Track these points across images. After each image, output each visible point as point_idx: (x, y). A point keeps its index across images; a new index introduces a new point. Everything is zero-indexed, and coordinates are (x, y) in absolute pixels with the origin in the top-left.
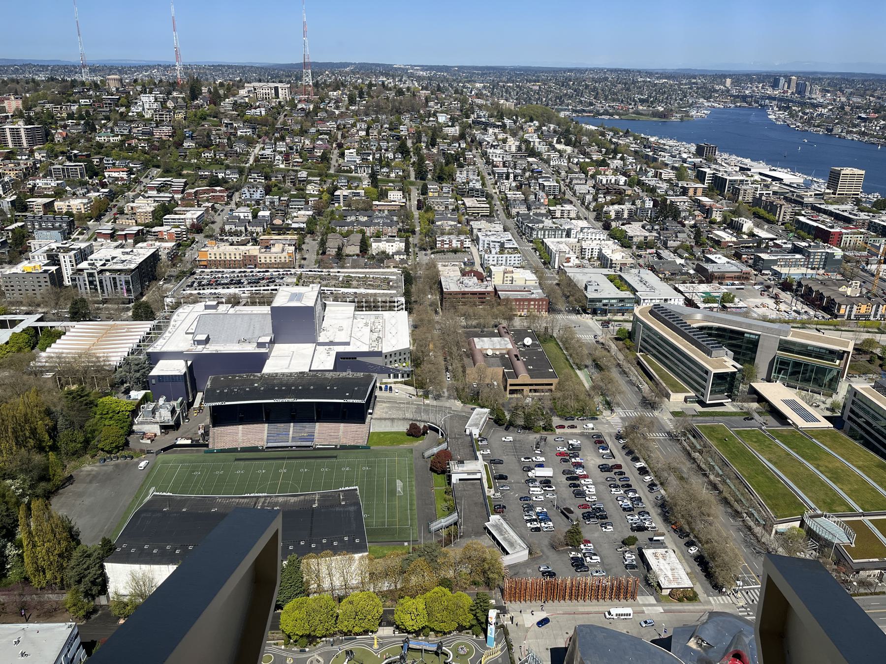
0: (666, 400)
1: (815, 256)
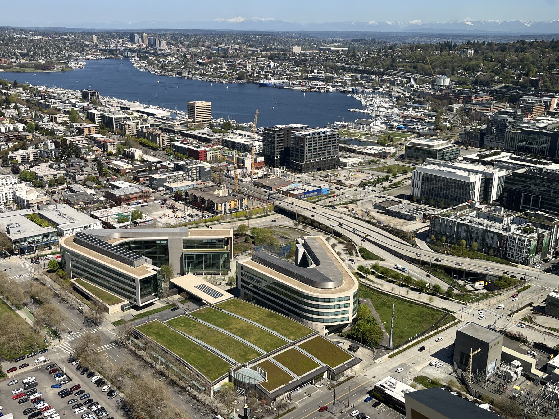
0: (106, 313)
1: (192, 170)
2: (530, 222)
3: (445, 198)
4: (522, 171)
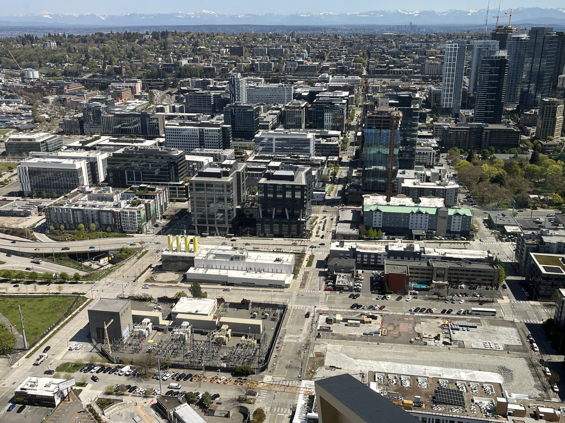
2: (137, 195)
3: (57, 188)
4: (120, 151)
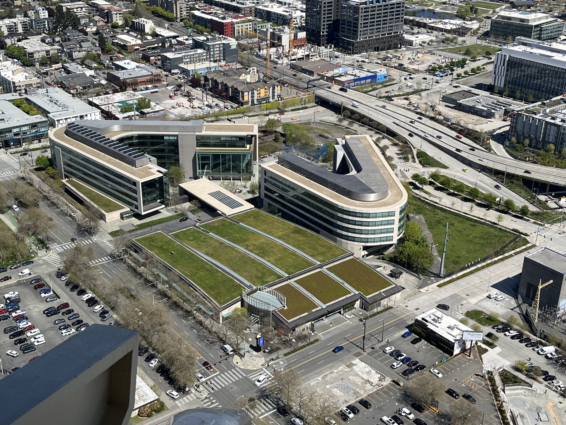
0: (102, 221)
1: (214, 48)
3: (535, 90)
